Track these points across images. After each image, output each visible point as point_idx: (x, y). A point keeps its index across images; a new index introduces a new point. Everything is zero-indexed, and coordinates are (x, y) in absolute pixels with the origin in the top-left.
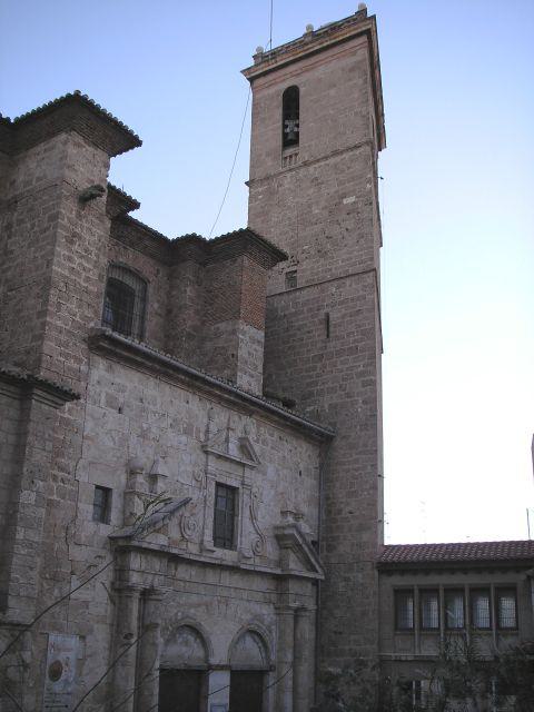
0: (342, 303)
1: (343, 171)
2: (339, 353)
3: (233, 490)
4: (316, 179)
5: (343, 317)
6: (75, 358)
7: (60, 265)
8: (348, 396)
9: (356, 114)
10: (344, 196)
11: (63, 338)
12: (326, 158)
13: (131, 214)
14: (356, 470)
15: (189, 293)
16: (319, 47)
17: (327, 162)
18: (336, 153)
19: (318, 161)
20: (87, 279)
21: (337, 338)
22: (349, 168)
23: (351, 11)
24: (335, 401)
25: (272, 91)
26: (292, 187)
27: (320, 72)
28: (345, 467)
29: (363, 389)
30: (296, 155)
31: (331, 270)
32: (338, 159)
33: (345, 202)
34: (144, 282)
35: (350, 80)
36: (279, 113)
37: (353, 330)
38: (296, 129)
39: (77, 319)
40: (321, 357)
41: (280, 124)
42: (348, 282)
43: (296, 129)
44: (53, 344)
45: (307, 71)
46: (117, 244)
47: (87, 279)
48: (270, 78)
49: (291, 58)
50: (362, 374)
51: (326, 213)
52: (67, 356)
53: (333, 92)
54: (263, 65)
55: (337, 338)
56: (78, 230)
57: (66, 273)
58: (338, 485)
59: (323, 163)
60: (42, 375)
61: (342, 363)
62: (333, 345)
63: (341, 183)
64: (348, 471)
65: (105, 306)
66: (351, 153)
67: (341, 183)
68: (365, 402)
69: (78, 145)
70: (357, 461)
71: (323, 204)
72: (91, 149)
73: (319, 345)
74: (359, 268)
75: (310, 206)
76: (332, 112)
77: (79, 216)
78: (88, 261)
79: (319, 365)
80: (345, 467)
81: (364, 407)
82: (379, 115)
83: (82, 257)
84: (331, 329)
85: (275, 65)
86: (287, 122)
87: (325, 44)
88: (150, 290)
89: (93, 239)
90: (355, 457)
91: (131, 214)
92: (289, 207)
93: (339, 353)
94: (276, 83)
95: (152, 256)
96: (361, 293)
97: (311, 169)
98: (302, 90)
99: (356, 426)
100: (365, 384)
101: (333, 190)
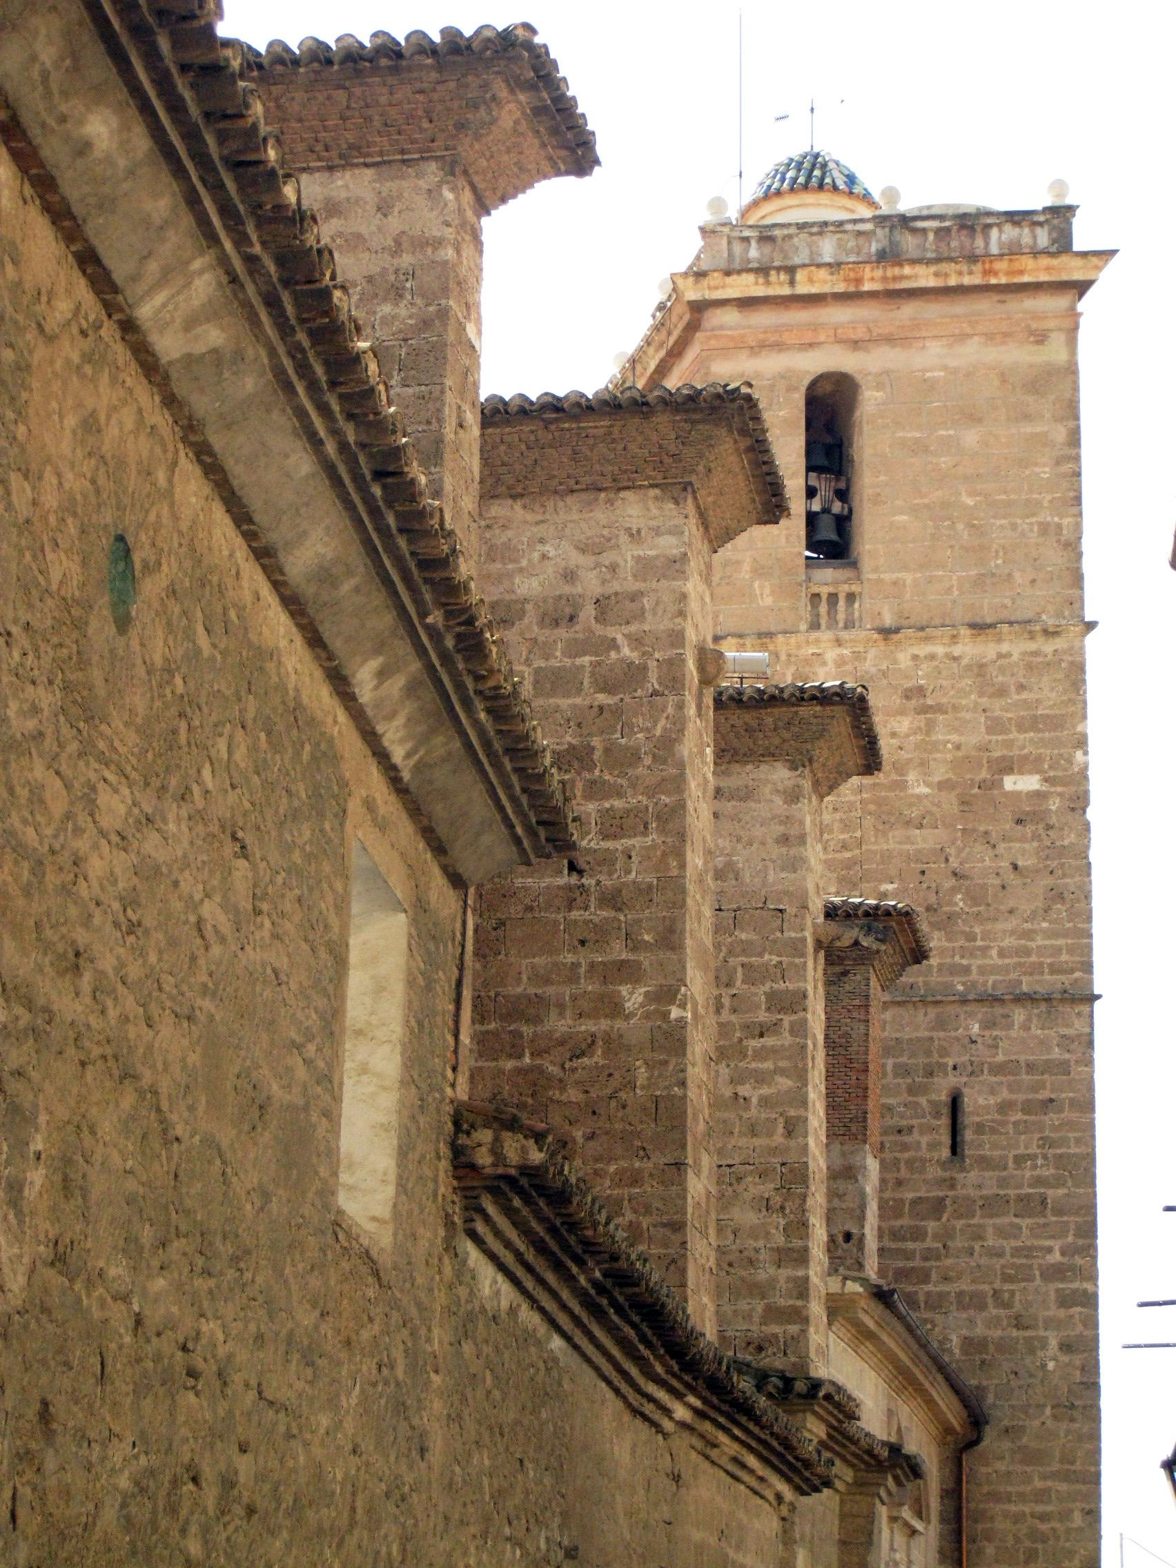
0: (997, 1069)
1: (1002, 692)
2: (993, 1205)
4: (921, 691)
5: (1005, 1107)
8: (1019, 1323)
9: (1044, 528)
10: (1007, 766)
14: (1043, 1518)
16: (932, 282)
21: (984, 1163)
22: (1021, 687)
23: (1036, 200)
24: (980, 1331)
28: (1013, 1508)
29: (1062, 1313)
30: (851, 597)
31: (966, 970)
32: (987, 649)
33: (1011, 783)
35: (1026, 417)
37: (1034, 1150)
38: (837, 507)
40: (938, 1207)
42: (1019, 1015)
43: (837, 507)
45: (889, 340)
48: (765, 318)
50: (1056, 1273)
51: (950, 803)
53: (971, 437)
54: (751, 278)
55: (984, 1163)
58: (990, 1550)
61: (1001, 1232)
62: (972, 1181)
63: (995, 726)
64: (1018, 1518)
67: (995, 726)
68: (1066, 1347)
70: (1041, 1496)
71: (940, 773)
73: (934, 1172)
74: (1049, 982)
76: (970, 502)
79: (931, 1226)
80: (1013, 1508)
81: (1065, 1359)
84: (968, 1135)
85: (786, 291)
90: (1038, 1484)
93: (993, 1205)
94: (779, 347)
96: (1056, 1053)
98: (870, 402)
99: (1040, 1407)
100: (1066, 1301)
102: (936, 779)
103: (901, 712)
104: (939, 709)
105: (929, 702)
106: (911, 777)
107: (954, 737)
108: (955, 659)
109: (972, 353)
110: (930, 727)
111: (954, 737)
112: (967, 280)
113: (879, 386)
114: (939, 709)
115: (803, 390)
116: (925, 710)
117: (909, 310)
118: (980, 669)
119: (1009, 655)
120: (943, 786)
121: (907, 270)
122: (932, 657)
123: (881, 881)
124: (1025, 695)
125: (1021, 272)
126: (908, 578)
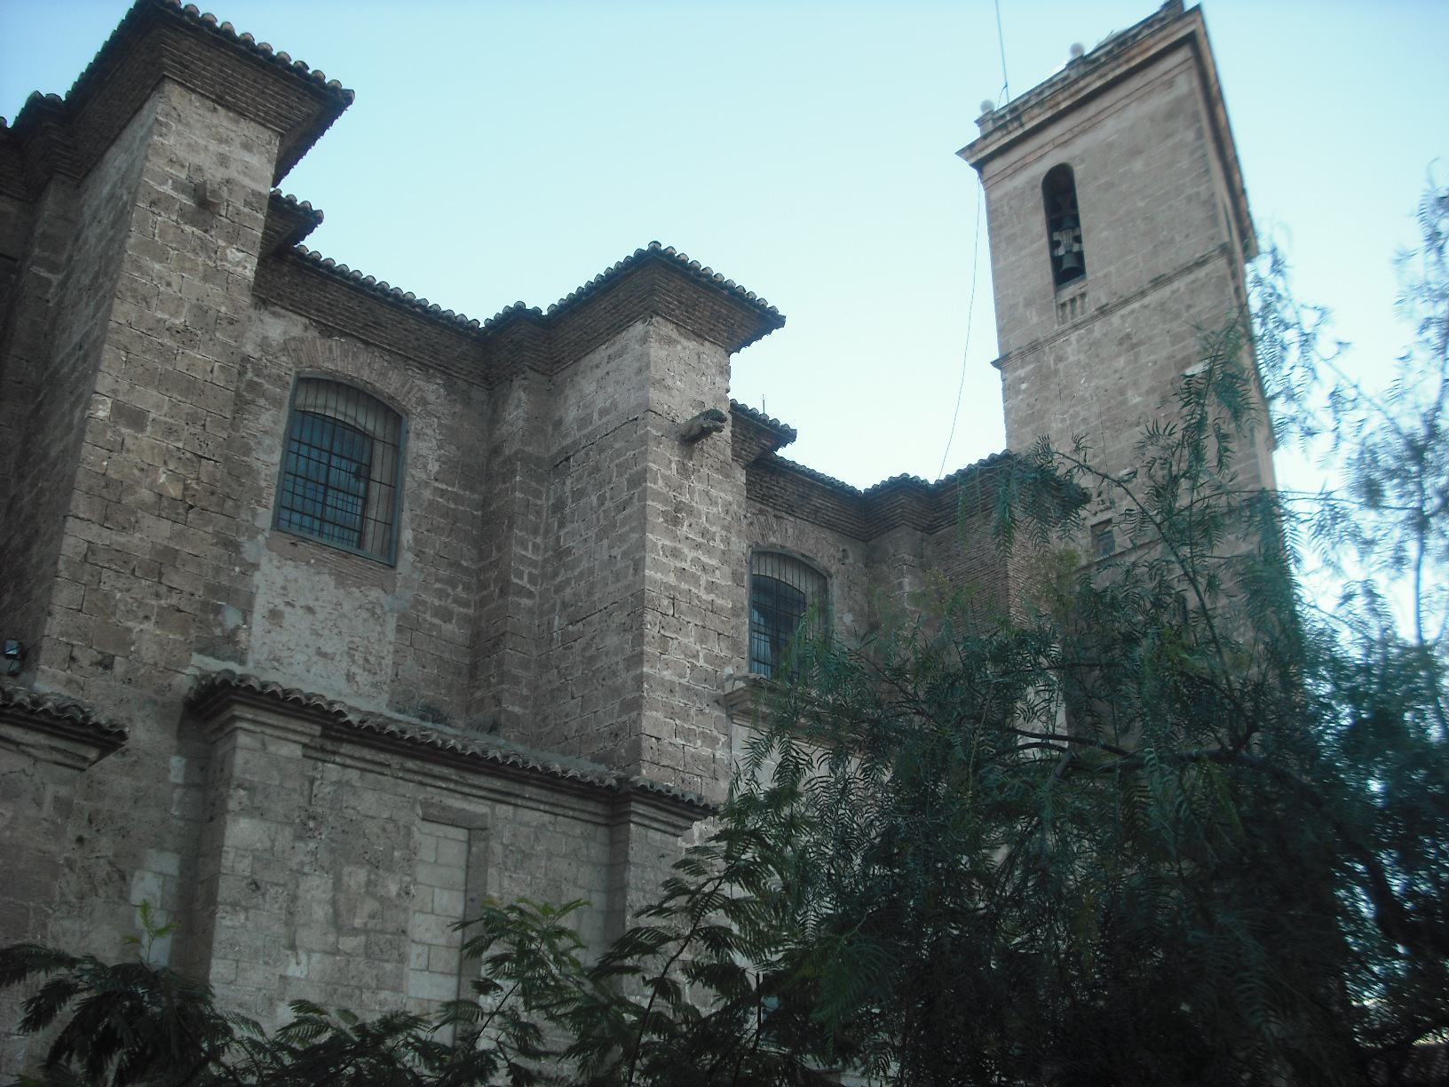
1: (1177, 315)
4: (1128, 336)
6: (704, 736)
7: (658, 566)
9: (1189, 199)
11: (678, 701)
12: (1143, 294)
13: (781, 452)
15: (907, 588)
17: (1146, 300)
18: (1159, 282)
19: (1126, 302)
20: (712, 587)
22: (1189, 307)
25: (1021, 179)
26: (1082, 357)
27: (1109, 129)
30: (1083, 295)
32: (1165, 292)
34: (822, 577)
35: (1168, 136)
36: (1038, 222)
38: (1076, 248)
39: (701, 663)
41: (1045, 241)
44: (660, 715)
45: (1084, 132)
46: (761, 512)
47: (712, 587)
49: (1049, 114)
52: (688, 735)
53: (1138, 165)
54: (998, 134)
56: (685, 498)
57: (671, 579)
59: (1136, 305)
60: (647, 774)
65: (752, 630)
66: (1191, 278)
69: (670, 341)
71: (1146, 384)
72: (692, 345)
75: (1122, 392)
76: (1142, 204)
77: (684, 471)
78: (710, 552)
82: (1237, 194)
83: (698, 546)
85: (1020, 132)
86: (1057, 237)
87: (1110, 77)
88: (836, 590)
89: (714, 510)
91: (781, 452)
92: (1083, 400)
95: (830, 526)
97: (1115, 319)
98: (1079, 173)
101: (1164, 353)
102: (1143, 390)
103: (1119, 355)
104: (1141, 343)
105: (1134, 341)
106: (1130, 393)
107: (1153, 357)
108: (1146, 307)
109: (1134, 113)
110: (1137, 356)
111: (1153, 357)
112: (1118, 72)
113: (1082, 161)
114: (1141, 343)
115: (1040, 185)
116: (1133, 346)
117: (1092, 109)
118: (1162, 306)
119: (1178, 289)
120: (1148, 393)
121: (1082, 84)
122: (1132, 312)
123: (1119, 470)
124: (1192, 311)
125: (1148, 49)
126: (1112, 268)
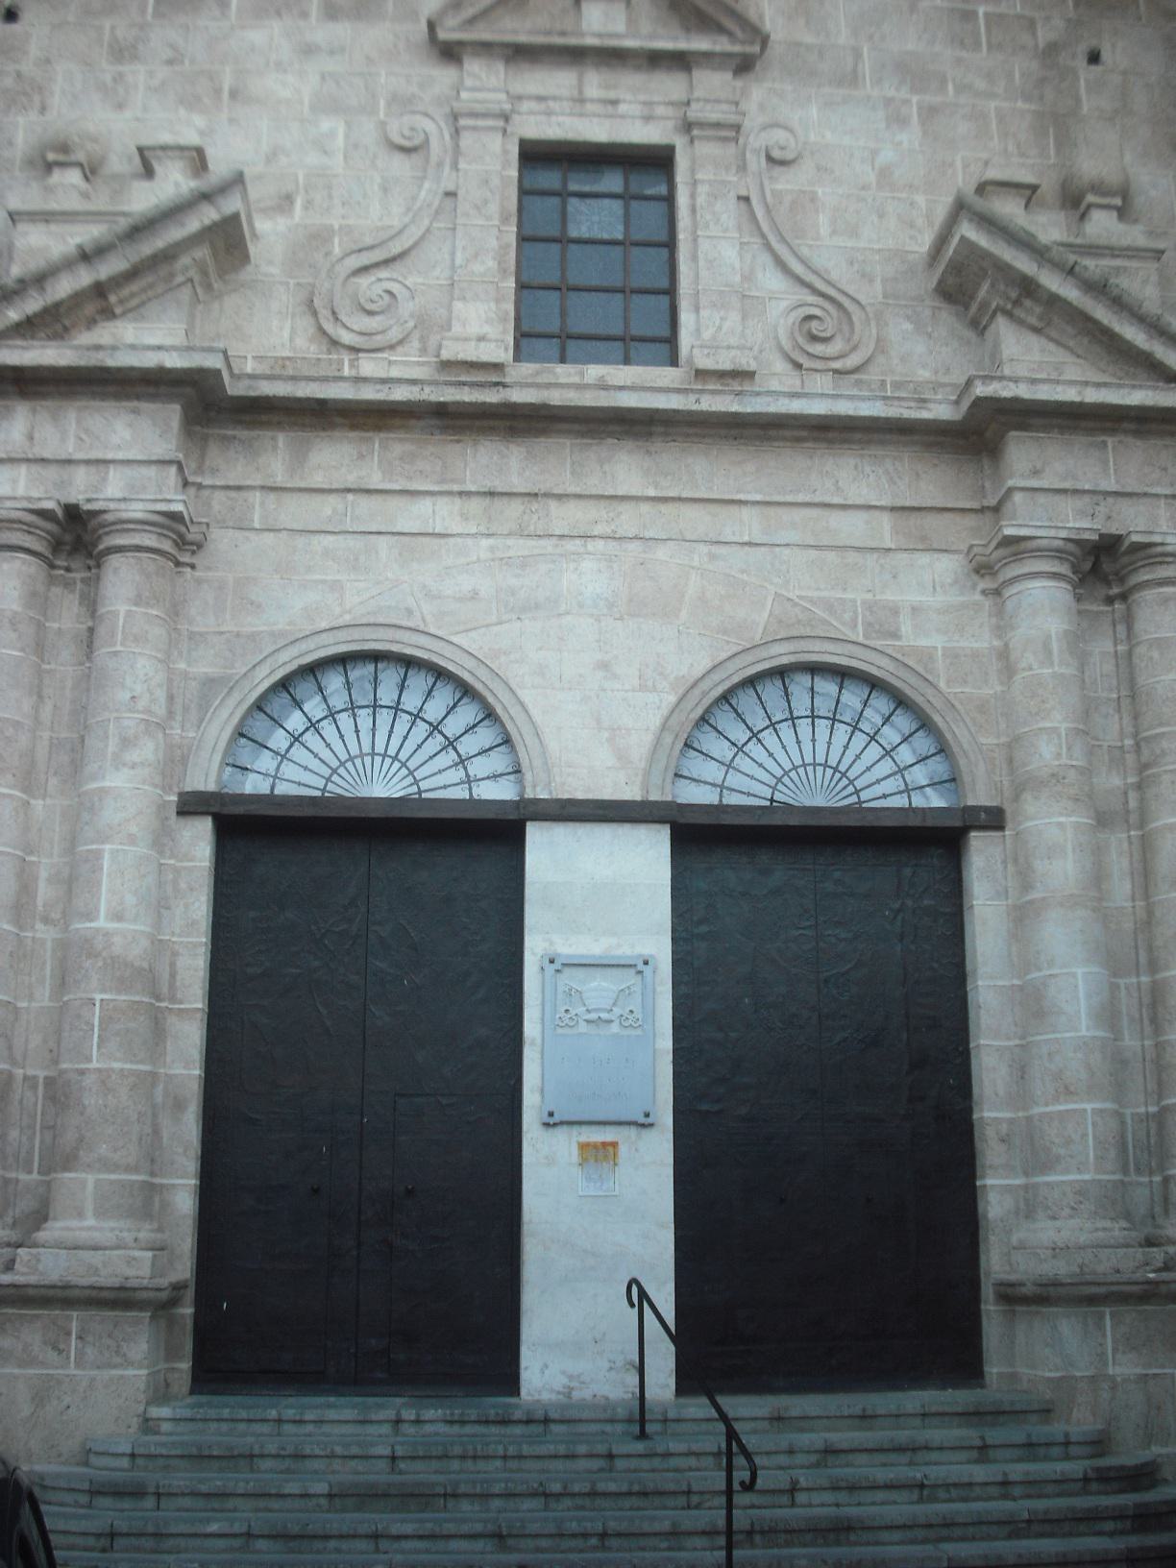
3: (657, 161)
